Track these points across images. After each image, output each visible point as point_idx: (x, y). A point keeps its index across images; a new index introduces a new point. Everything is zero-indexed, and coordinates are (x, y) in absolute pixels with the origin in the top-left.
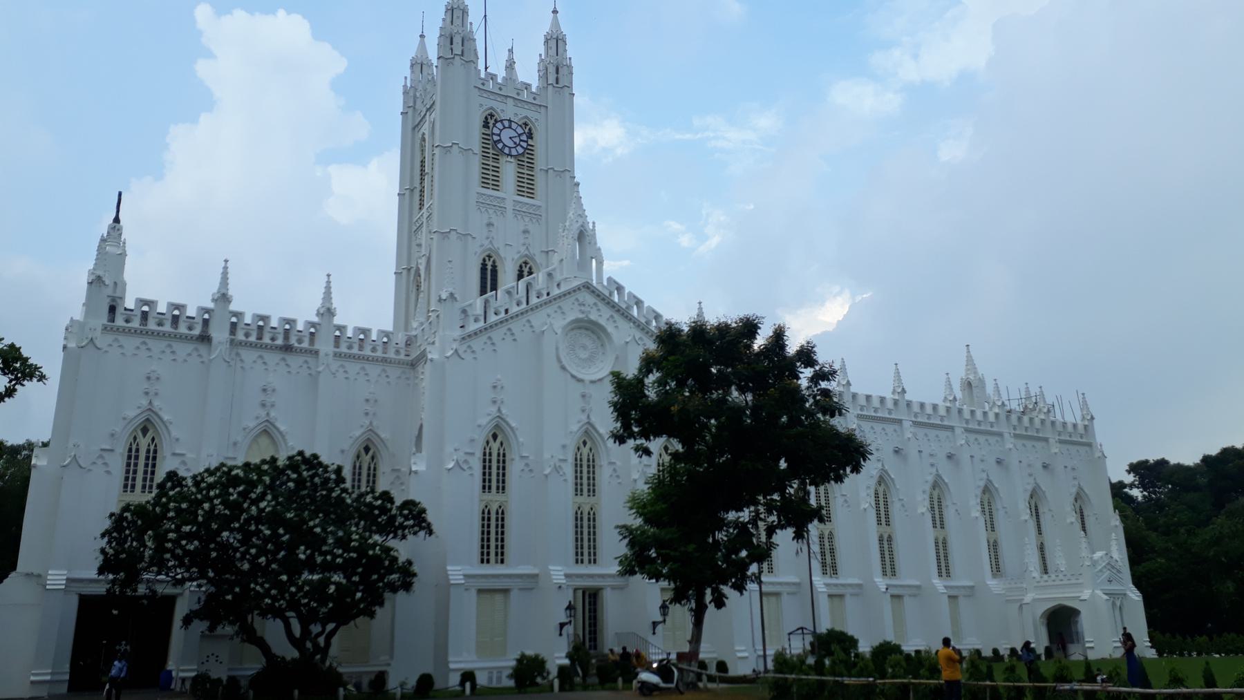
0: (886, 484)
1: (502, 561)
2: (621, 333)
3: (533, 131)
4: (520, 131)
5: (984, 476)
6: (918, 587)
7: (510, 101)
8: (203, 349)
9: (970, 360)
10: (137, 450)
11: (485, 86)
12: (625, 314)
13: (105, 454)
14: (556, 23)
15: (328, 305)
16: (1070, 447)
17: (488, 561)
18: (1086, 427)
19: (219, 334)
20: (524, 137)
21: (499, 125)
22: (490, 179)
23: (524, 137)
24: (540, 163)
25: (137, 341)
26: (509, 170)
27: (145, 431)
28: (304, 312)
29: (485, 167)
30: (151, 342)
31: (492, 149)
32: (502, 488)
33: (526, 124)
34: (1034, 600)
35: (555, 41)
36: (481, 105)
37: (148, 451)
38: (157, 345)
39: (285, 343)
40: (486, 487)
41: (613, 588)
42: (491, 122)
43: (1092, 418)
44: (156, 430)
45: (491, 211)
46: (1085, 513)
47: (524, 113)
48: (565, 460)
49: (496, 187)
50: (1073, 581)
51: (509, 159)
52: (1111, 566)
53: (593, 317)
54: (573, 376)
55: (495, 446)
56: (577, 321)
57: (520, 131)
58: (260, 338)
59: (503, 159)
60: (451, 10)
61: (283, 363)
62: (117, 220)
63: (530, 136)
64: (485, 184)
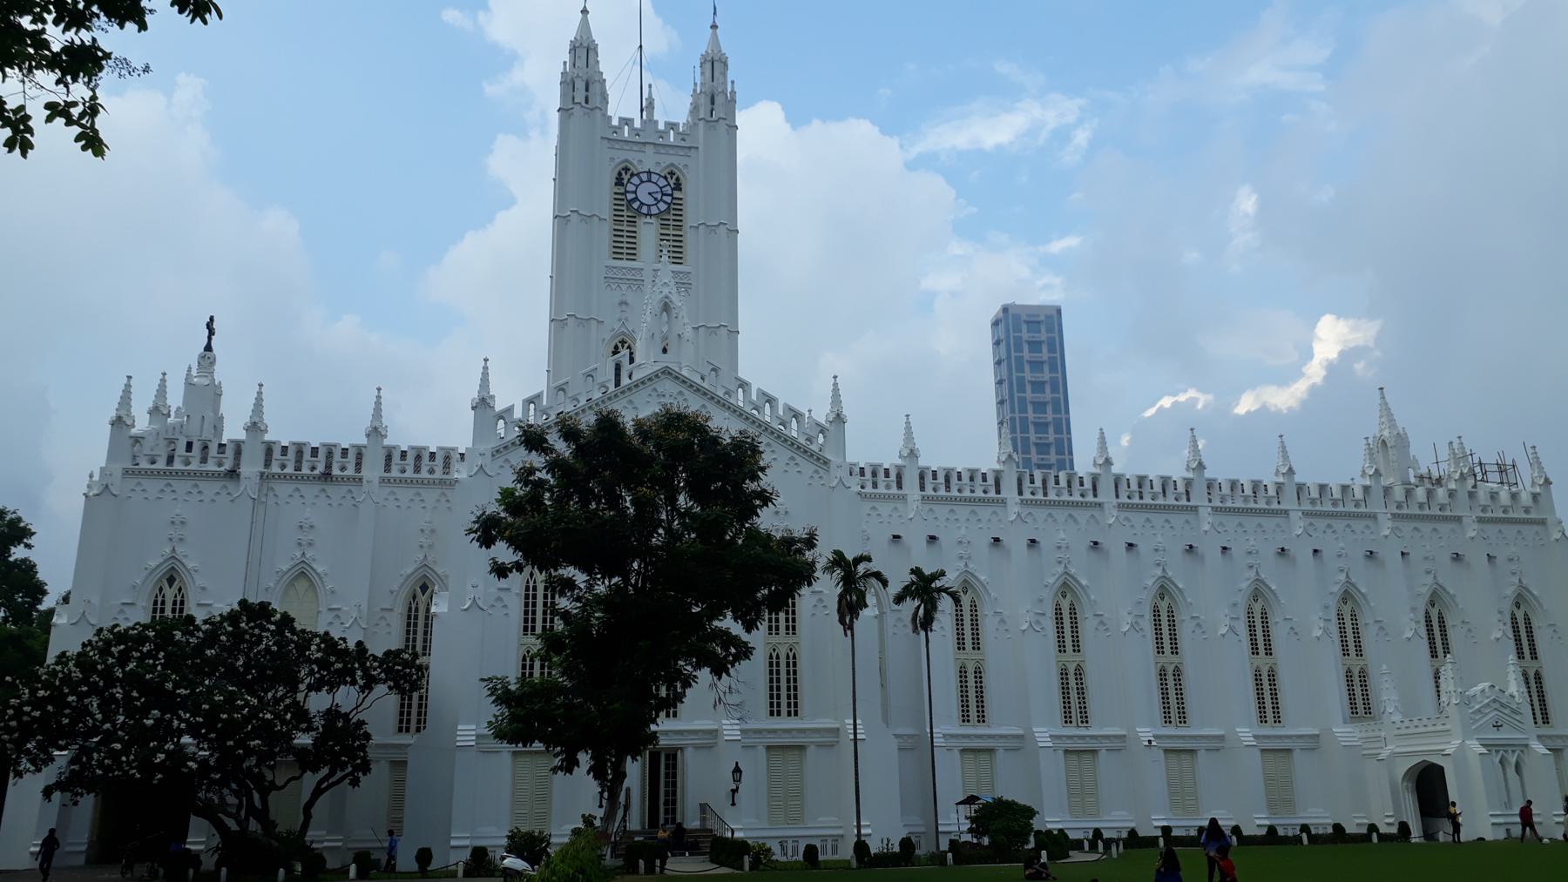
0: (1172, 597)
3: (682, 180)
4: (662, 182)
5: (1342, 577)
6: (1221, 738)
7: (650, 150)
8: (231, 485)
9: (1385, 408)
10: (163, 603)
11: (612, 137)
13: (126, 608)
14: (715, 40)
15: (377, 424)
16: (1503, 527)
17: (779, 714)
18: (1535, 497)
19: (251, 468)
20: (668, 190)
21: (635, 180)
22: (624, 247)
23: (668, 190)
24: (691, 217)
25: (161, 483)
26: (648, 232)
27: (171, 581)
28: (352, 435)
29: (617, 233)
30: (176, 484)
31: (627, 209)
33: (672, 174)
34: (1395, 755)
35: (714, 64)
37: (175, 603)
38: (181, 486)
39: (323, 468)
41: (697, 747)
42: (626, 178)
43: (1547, 482)
44: (182, 580)
45: (624, 287)
46: (1535, 624)
49: (632, 256)
50: (1440, 728)
51: (648, 219)
52: (1499, 704)
58: (298, 468)
59: (641, 221)
60: (574, 49)
61: (323, 496)
62: (208, 348)
63: (678, 187)
64: (617, 255)
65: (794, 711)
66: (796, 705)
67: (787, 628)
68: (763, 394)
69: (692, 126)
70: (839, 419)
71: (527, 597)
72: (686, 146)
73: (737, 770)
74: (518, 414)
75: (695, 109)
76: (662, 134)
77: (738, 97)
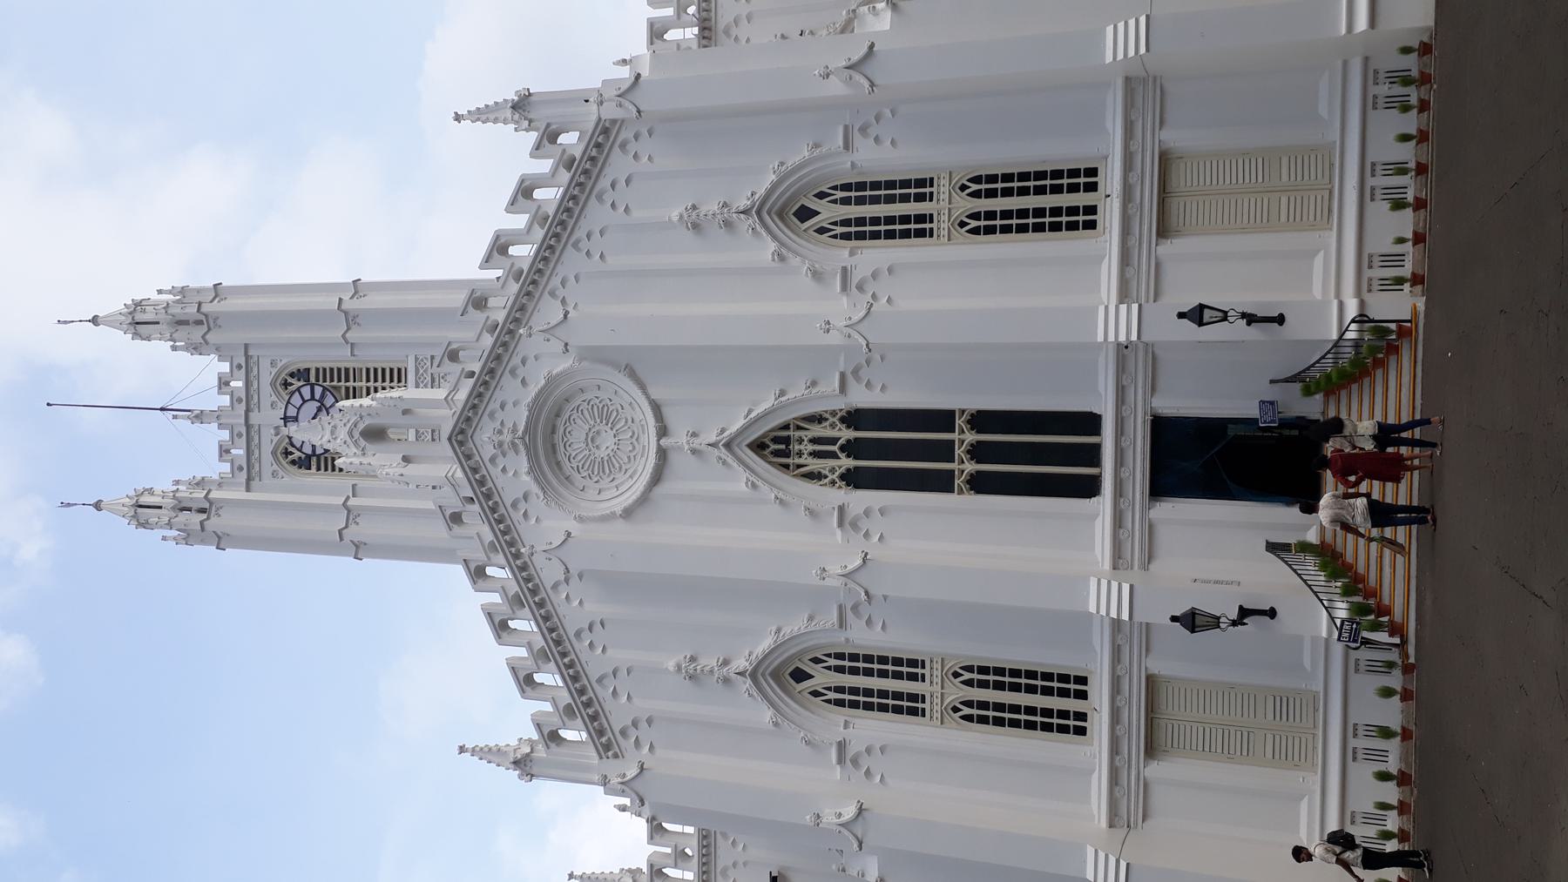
1: (1082, 680)
2: (543, 360)
3: (293, 368)
4: (296, 400)
12: (507, 336)
20: (306, 391)
32: (911, 667)
35: (138, 321)
36: (274, 474)
40: (911, 706)
47: (266, 389)
48: (842, 510)
53: (521, 417)
54: (657, 478)
55: (822, 678)
56: (535, 469)
57: (296, 400)
60: (144, 525)
63: (302, 374)
65: (1086, 178)
66: (1074, 173)
67: (920, 198)
68: (487, 262)
69: (221, 352)
70: (522, 106)
71: (854, 705)
72: (247, 365)
73: (1197, 315)
74: (547, 707)
75: (195, 349)
76: (235, 399)
77: (179, 284)
